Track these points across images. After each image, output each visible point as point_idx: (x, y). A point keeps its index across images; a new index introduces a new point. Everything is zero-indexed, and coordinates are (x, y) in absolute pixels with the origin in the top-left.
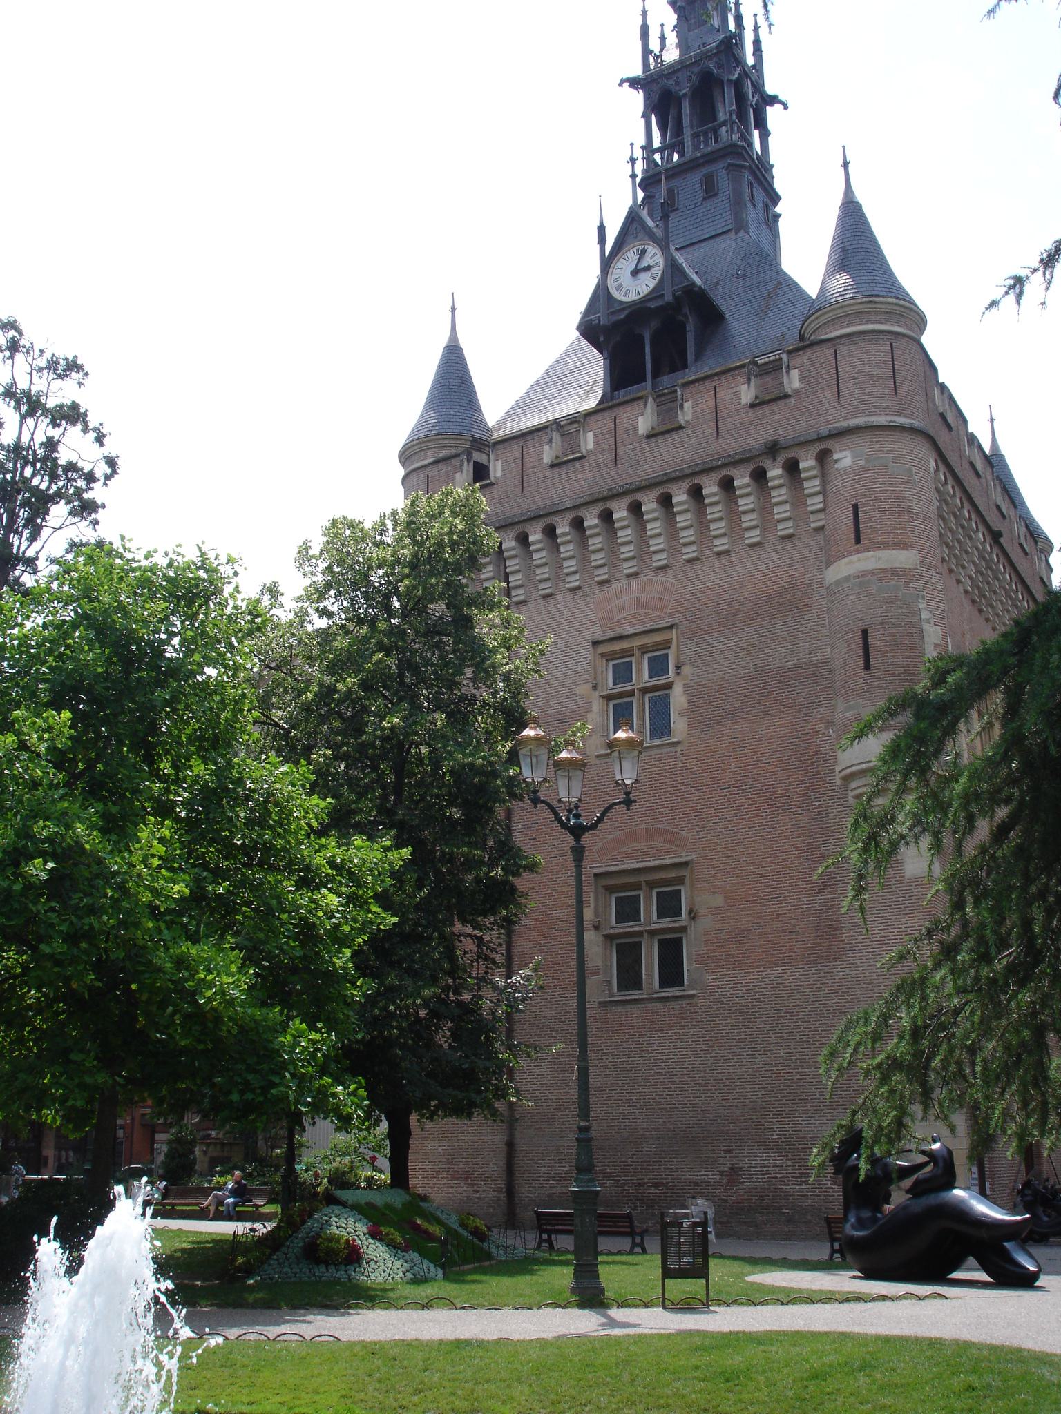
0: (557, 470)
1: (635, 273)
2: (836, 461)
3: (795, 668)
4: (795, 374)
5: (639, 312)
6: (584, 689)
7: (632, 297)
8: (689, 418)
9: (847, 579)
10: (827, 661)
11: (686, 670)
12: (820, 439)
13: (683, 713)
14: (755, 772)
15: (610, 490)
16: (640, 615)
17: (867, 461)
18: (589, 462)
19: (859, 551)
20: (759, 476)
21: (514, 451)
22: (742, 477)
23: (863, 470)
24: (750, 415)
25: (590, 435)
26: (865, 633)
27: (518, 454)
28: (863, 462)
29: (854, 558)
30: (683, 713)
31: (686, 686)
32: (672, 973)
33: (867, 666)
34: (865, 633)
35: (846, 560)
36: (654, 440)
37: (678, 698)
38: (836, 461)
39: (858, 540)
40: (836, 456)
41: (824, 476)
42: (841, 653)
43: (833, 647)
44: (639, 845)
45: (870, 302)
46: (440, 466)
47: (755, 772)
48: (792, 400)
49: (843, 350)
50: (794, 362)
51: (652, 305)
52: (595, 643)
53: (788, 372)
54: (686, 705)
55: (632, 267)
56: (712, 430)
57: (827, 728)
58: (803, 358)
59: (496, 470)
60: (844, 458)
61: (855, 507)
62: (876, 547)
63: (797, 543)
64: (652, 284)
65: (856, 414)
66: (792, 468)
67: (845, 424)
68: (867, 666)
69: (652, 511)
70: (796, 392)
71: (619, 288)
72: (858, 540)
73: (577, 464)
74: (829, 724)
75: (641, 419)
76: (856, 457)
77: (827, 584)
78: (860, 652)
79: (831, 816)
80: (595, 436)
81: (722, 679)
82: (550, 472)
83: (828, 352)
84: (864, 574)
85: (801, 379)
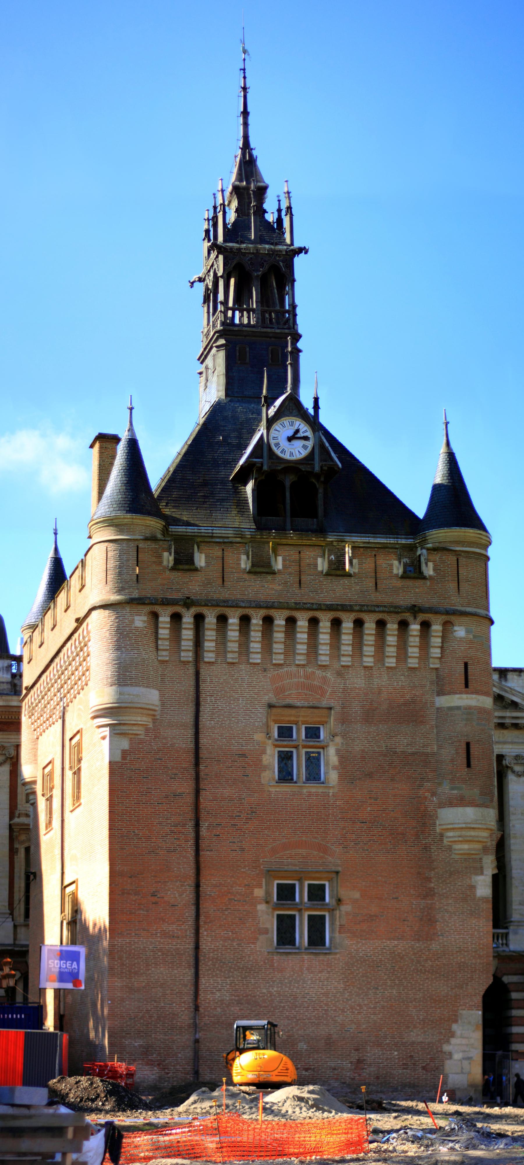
0: (252, 577)
1: (290, 439)
2: (455, 631)
3: (413, 754)
4: (431, 565)
5: (292, 467)
6: (259, 737)
7: (287, 457)
8: (356, 571)
9: (458, 708)
10: (434, 754)
11: (338, 739)
12: (447, 613)
13: (335, 768)
14: (384, 815)
15: (296, 603)
16: (306, 695)
17: (474, 637)
18: (278, 577)
19: (467, 693)
20: (403, 625)
21: (217, 552)
22: (393, 623)
23: (471, 642)
24: (399, 583)
25: (280, 559)
26: (468, 744)
27: (220, 554)
28: (471, 637)
29: (464, 696)
30: (335, 768)
31: (338, 751)
32: (317, 937)
33: (469, 765)
34: (468, 744)
35: (457, 696)
36: (330, 577)
37: (331, 756)
38: (455, 631)
39: (467, 686)
40: (456, 628)
41: (444, 638)
42: (450, 754)
43: (440, 747)
44: (300, 851)
45: (480, 534)
46: (149, 543)
47: (384, 815)
48: (428, 583)
49: (462, 561)
50: (431, 557)
51: (303, 468)
52: (271, 706)
53: (426, 564)
54: (337, 763)
55: (290, 433)
56: (372, 584)
57: (432, 796)
58: (437, 557)
59: (200, 560)
60: (460, 632)
61: (466, 665)
62: (477, 692)
63: (418, 673)
64: (304, 453)
65: (469, 605)
66: (426, 625)
67: (463, 609)
68: (469, 765)
69: (325, 628)
70: (431, 578)
71: (277, 445)
72: (467, 686)
73: (269, 577)
74: (434, 794)
75: (320, 560)
76: (468, 631)
77: (437, 705)
78: (465, 755)
79: (432, 851)
80: (284, 560)
81: (363, 751)
82: (246, 576)
83: (451, 559)
84: (470, 708)
85: (435, 570)
